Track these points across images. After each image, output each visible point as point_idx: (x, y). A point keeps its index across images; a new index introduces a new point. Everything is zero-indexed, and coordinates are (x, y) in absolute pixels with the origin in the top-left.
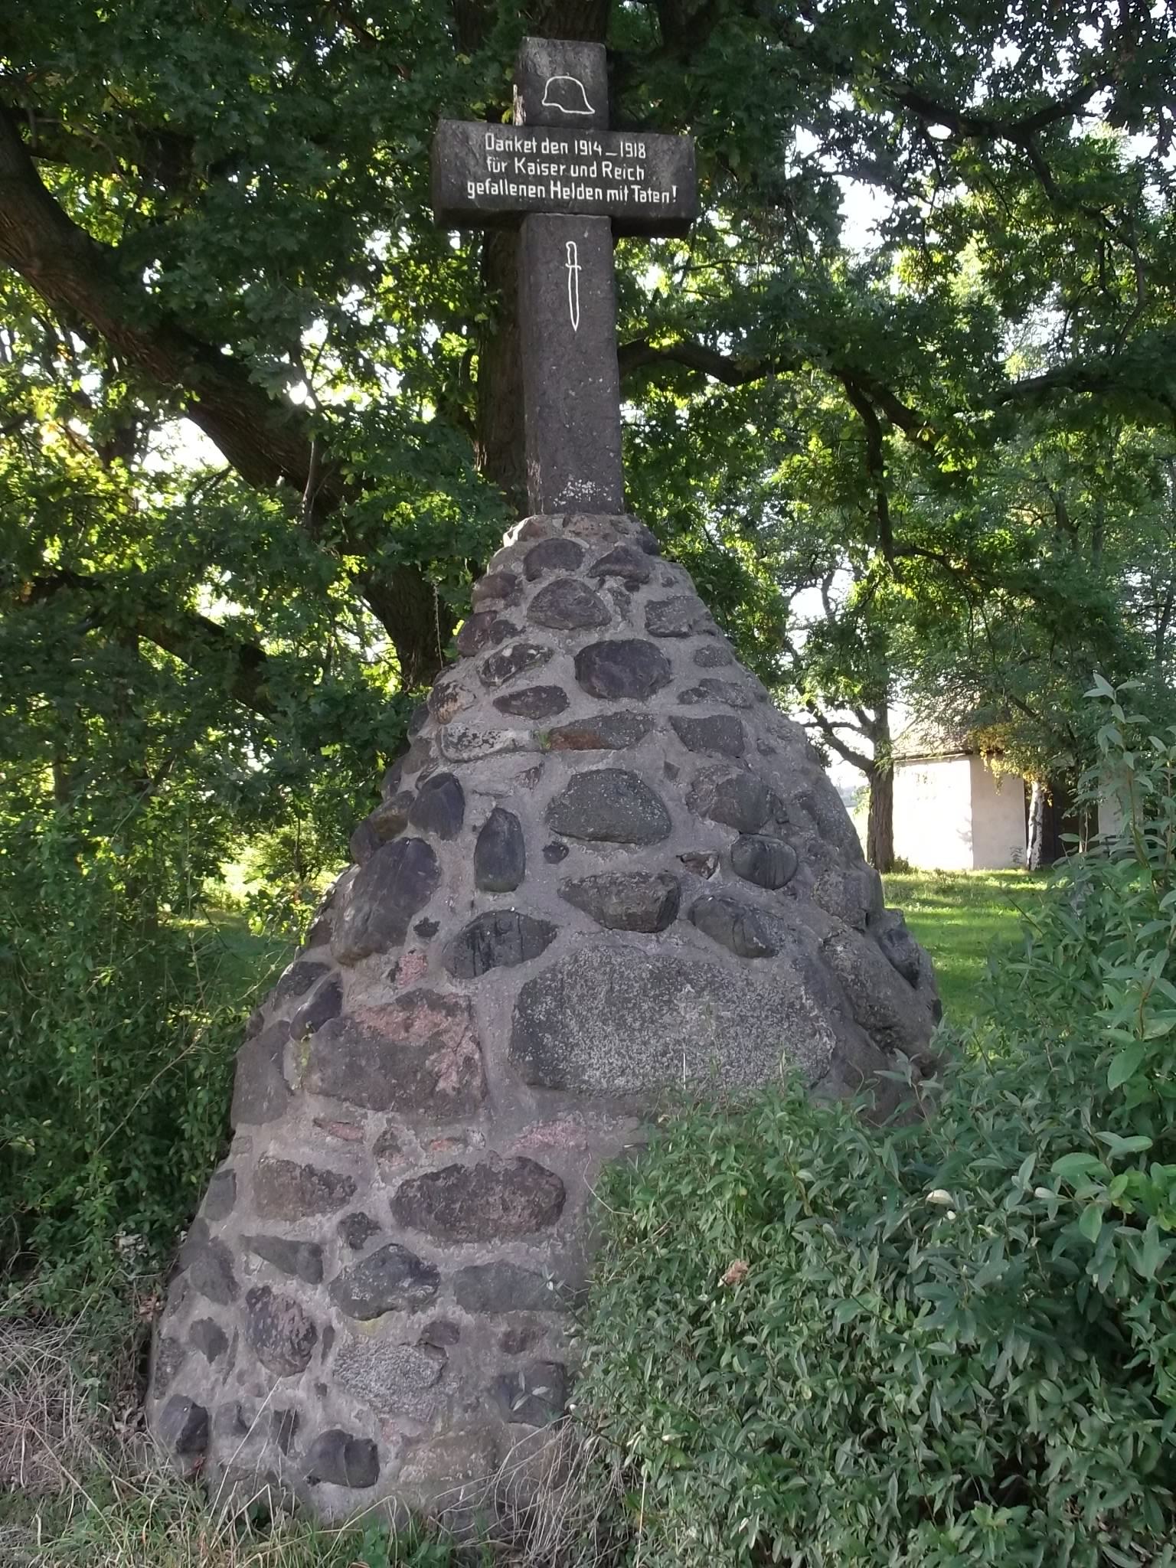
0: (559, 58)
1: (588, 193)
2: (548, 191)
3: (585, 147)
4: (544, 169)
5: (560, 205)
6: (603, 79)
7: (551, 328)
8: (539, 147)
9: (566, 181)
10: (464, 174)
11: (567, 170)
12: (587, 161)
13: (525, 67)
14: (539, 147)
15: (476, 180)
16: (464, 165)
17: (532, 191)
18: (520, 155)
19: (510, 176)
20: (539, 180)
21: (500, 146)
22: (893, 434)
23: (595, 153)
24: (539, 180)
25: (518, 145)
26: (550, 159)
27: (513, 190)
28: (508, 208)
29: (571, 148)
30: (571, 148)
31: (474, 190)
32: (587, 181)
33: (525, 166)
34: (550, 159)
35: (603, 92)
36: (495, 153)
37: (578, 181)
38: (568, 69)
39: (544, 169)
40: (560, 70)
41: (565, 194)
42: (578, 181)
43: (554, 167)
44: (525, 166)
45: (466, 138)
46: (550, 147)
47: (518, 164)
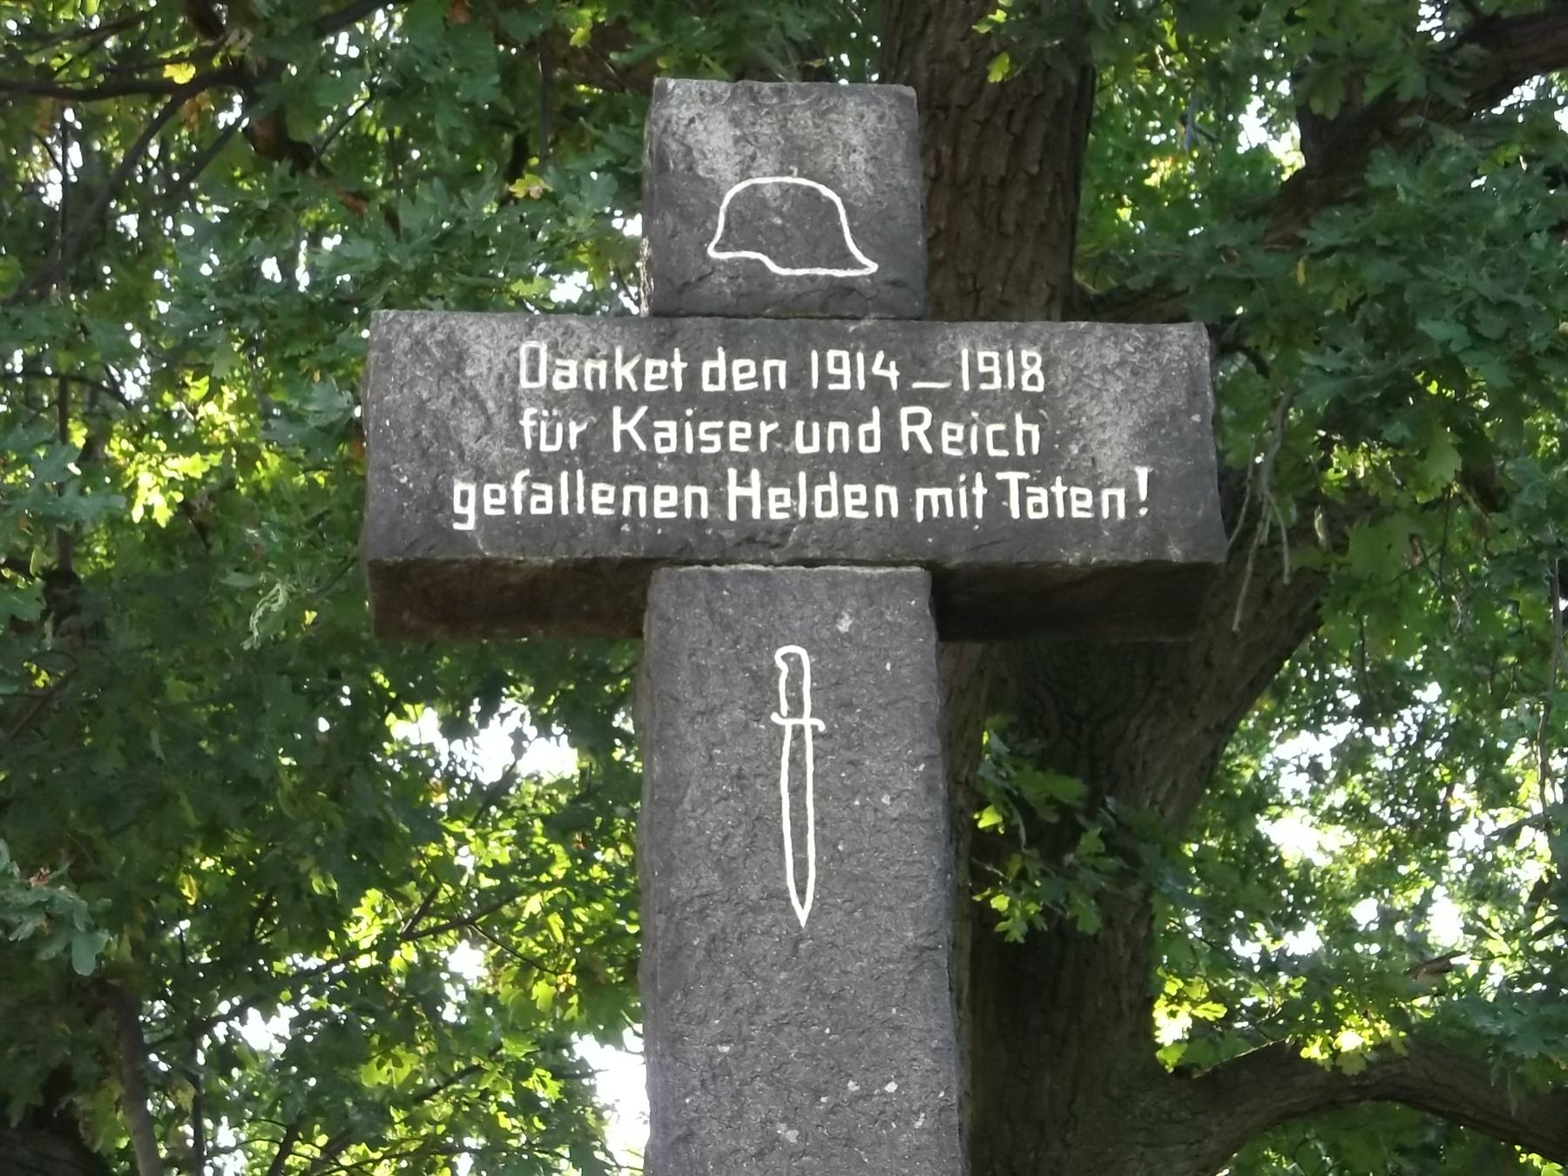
0: (766, 129)
1: (850, 501)
2: (718, 500)
3: (843, 368)
4: (707, 436)
5: (758, 539)
6: (907, 179)
7: (719, 917)
8: (692, 376)
9: (780, 468)
10: (439, 456)
11: (785, 435)
12: (851, 408)
13: (661, 161)
14: (692, 376)
15: (481, 475)
16: (444, 432)
17: (665, 501)
18: (630, 401)
19: (593, 458)
20: (688, 468)
21: (567, 376)
22: (439, 805)
23: (877, 386)
24: (688, 468)
25: (624, 372)
26: (730, 406)
27: (601, 499)
28: (582, 552)
29: (798, 375)
30: (798, 375)
31: (472, 505)
32: (851, 466)
33: (646, 430)
34: (730, 406)
35: (907, 215)
36: (552, 399)
37: (818, 467)
38: (794, 154)
39: (707, 436)
40: (767, 161)
41: (777, 505)
42: (818, 467)
43: (739, 429)
44: (646, 430)
45: (458, 357)
46: (729, 372)
47: (620, 425)
